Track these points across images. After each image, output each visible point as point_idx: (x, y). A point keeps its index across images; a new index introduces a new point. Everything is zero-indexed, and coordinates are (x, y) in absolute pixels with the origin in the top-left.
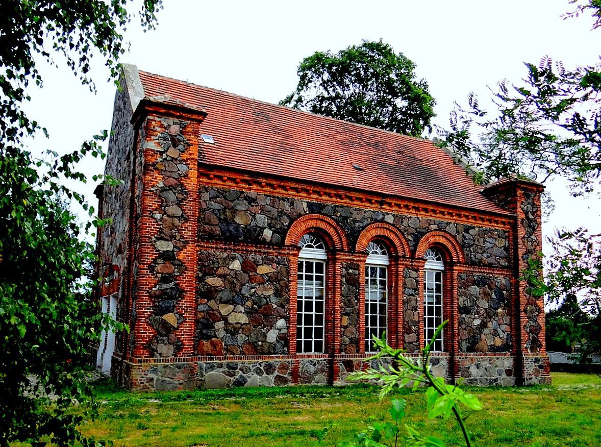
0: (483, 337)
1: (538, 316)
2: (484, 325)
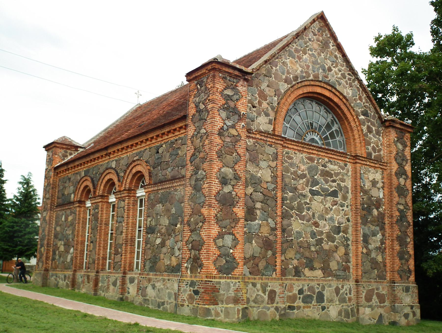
0: (162, 256)
1: (201, 227)
2: (163, 244)
